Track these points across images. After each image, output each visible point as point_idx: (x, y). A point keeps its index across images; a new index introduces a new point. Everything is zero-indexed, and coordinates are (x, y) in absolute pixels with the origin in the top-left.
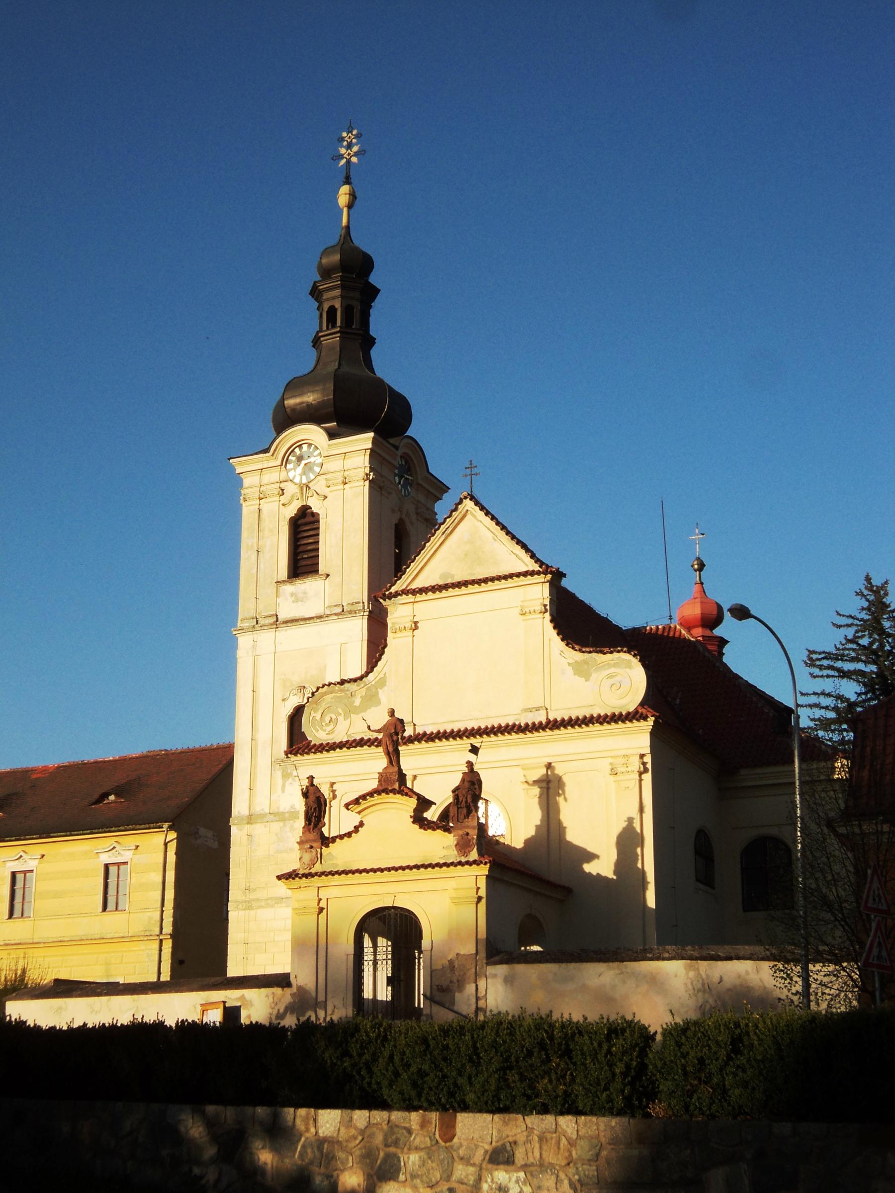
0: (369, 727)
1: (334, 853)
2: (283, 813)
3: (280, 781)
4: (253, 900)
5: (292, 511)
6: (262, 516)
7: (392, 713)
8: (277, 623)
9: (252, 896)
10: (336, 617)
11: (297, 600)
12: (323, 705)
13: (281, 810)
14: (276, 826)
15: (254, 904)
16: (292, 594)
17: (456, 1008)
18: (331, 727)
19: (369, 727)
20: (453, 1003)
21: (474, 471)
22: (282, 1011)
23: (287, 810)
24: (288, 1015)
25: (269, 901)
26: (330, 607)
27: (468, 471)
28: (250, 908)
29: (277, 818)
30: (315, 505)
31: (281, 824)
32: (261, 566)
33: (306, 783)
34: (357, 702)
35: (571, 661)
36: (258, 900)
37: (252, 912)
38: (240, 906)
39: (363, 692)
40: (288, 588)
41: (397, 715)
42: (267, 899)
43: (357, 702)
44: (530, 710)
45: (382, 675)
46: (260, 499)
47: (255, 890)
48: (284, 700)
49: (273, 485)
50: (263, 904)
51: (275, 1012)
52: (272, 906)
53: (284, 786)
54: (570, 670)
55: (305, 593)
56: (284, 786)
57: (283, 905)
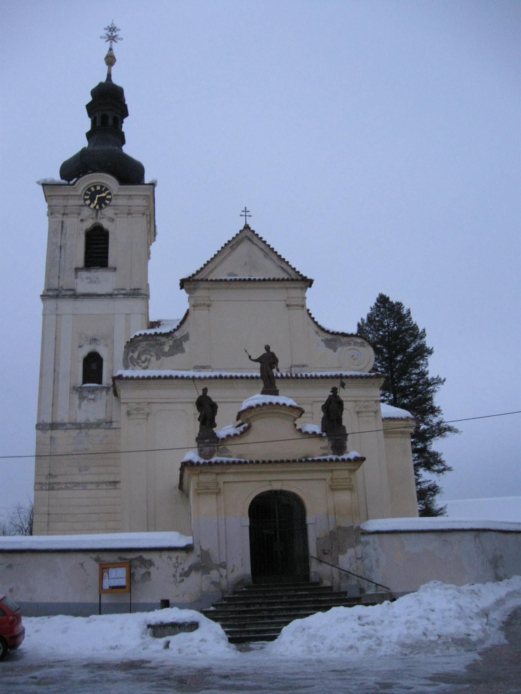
0: (250, 357)
1: (228, 447)
2: (80, 424)
3: (77, 402)
4: (55, 483)
5: (88, 224)
6: (65, 225)
7: (267, 348)
8: (75, 296)
9: (52, 481)
10: (123, 296)
11: (91, 282)
12: (140, 349)
13: (78, 421)
14: (74, 433)
15: (56, 487)
16: (87, 278)
17: (341, 567)
18: (146, 364)
19: (250, 357)
20: (337, 563)
21: (248, 214)
22: (186, 569)
23: (83, 421)
24: (193, 574)
25: (68, 485)
26: (118, 289)
27: (244, 214)
28: (53, 489)
29: (74, 427)
30: (106, 224)
31: (78, 431)
32: (63, 256)
33: (201, 393)
34: (166, 349)
35: (323, 338)
36: (59, 483)
37: (54, 492)
38: (44, 487)
39: (171, 342)
40: (84, 274)
41: (272, 350)
42: (67, 483)
43: (166, 349)
44: (298, 366)
45: (185, 333)
46: (64, 214)
47: (56, 476)
48: (80, 347)
49: (74, 207)
50: (63, 486)
51: (179, 570)
52: (71, 489)
53: (80, 405)
54: (323, 344)
55: (97, 278)
56: (80, 405)
57: (80, 488)
